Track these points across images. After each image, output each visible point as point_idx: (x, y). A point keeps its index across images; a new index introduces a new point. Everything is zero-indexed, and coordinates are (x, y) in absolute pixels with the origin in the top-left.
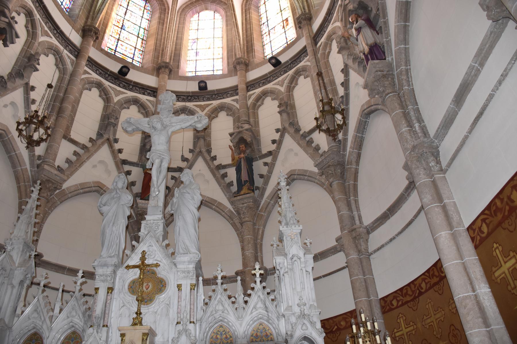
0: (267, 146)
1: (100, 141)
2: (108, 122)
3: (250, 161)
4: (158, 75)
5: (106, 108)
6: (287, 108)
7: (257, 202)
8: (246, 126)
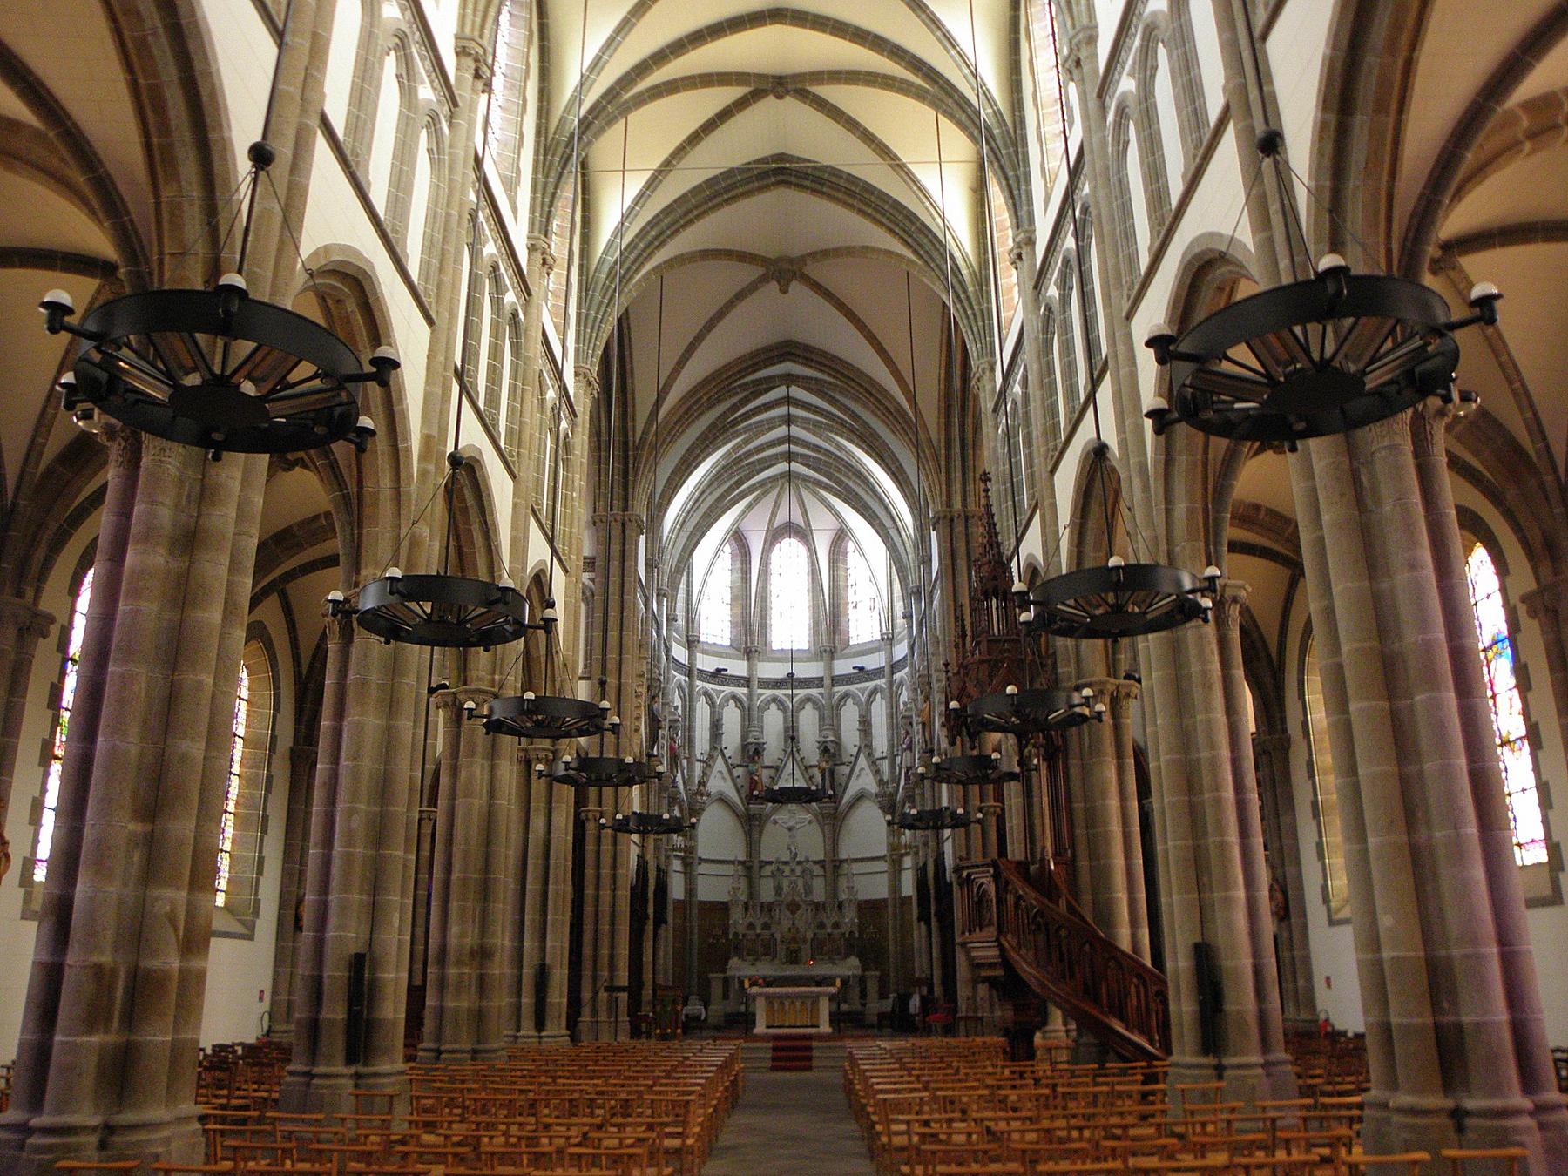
0: (846, 759)
1: (715, 753)
3: (832, 772)
5: (712, 713)
6: (865, 724)
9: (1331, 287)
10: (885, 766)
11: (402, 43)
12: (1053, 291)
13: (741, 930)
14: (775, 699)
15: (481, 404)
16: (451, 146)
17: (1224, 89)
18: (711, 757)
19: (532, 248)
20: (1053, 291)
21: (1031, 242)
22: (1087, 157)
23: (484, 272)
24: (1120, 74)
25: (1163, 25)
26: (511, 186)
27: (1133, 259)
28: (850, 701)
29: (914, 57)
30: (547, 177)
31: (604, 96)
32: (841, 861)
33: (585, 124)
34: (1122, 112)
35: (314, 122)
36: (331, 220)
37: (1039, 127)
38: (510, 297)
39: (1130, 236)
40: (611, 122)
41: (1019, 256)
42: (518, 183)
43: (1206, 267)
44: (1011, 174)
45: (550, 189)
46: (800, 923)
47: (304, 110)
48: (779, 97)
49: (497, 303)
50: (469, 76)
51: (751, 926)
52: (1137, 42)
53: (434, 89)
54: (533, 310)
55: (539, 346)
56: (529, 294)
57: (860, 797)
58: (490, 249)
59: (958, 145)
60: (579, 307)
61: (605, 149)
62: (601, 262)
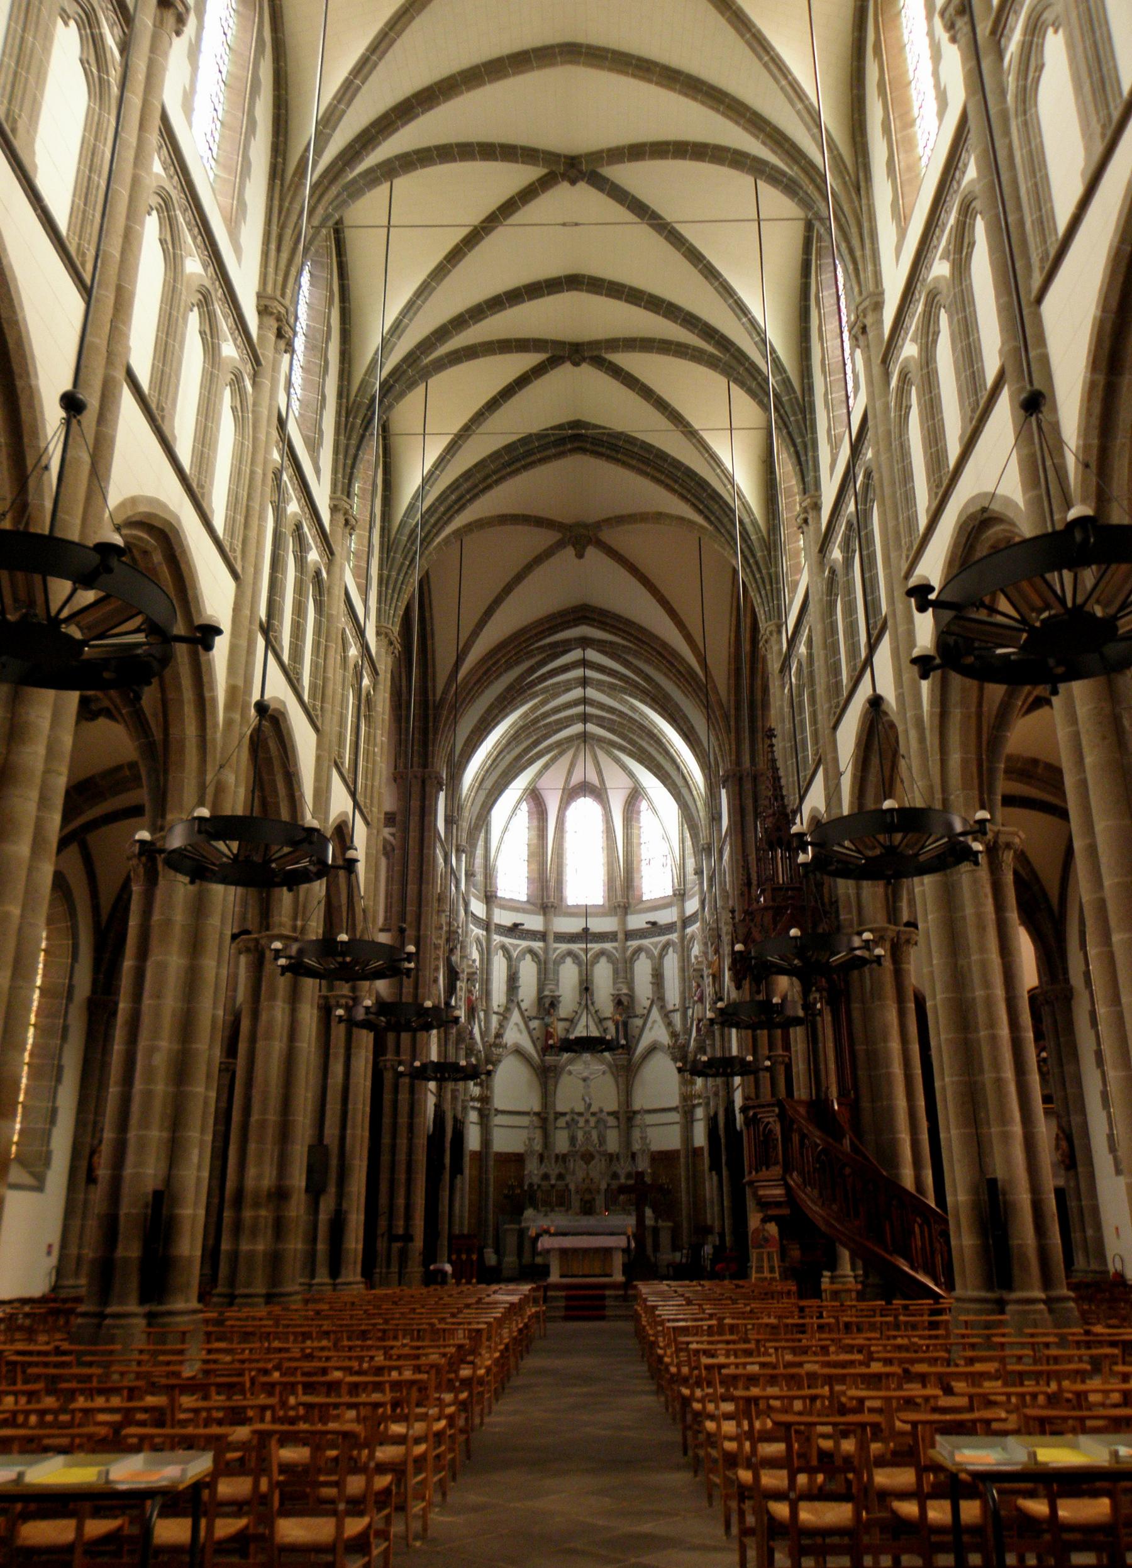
0: (639, 1011)
1: (512, 1006)
2: (513, 980)
3: (625, 1024)
4: (545, 914)
5: (509, 967)
6: (658, 977)
7: (630, 1060)
8: (625, 991)
9: (1078, 536)
10: (677, 1018)
11: (205, 302)
12: (837, 554)
13: (536, 1180)
14: (570, 953)
15: (285, 658)
16: (255, 405)
17: (1000, 352)
18: (508, 1009)
19: (334, 509)
20: (837, 554)
21: (817, 507)
22: (870, 423)
23: (288, 530)
24: (904, 340)
25: (945, 291)
26: (314, 447)
27: (912, 521)
28: (643, 955)
29: (706, 325)
30: (349, 439)
31: (405, 360)
32: (635, 1113)
33: (387, 387)
34: (904, 377)
35: (120, 375)
36: (137, 472)
37: (826, 394)
38: (313, 556)
39: (909, 498)
40: (412, 385)
41: (806, 521)
42: (320, 444)
43: (981, 522)
44: (798, 441)
45: (352, 451)
46: (595, 1174)
47: (110, 361)
48: (576, 364)
49: (301, 561)
50: (272, 336)
51: (546, 1177)
52: (920, 308)
53: (237, 347)
54: (336, 569)
55: (342, 605)
56: (332, 553)
57: (653, 1048)
58: (294, 507)
59: (747, 410)
60: (381, 568)
61: (408, 411)
62: (403, 524)
